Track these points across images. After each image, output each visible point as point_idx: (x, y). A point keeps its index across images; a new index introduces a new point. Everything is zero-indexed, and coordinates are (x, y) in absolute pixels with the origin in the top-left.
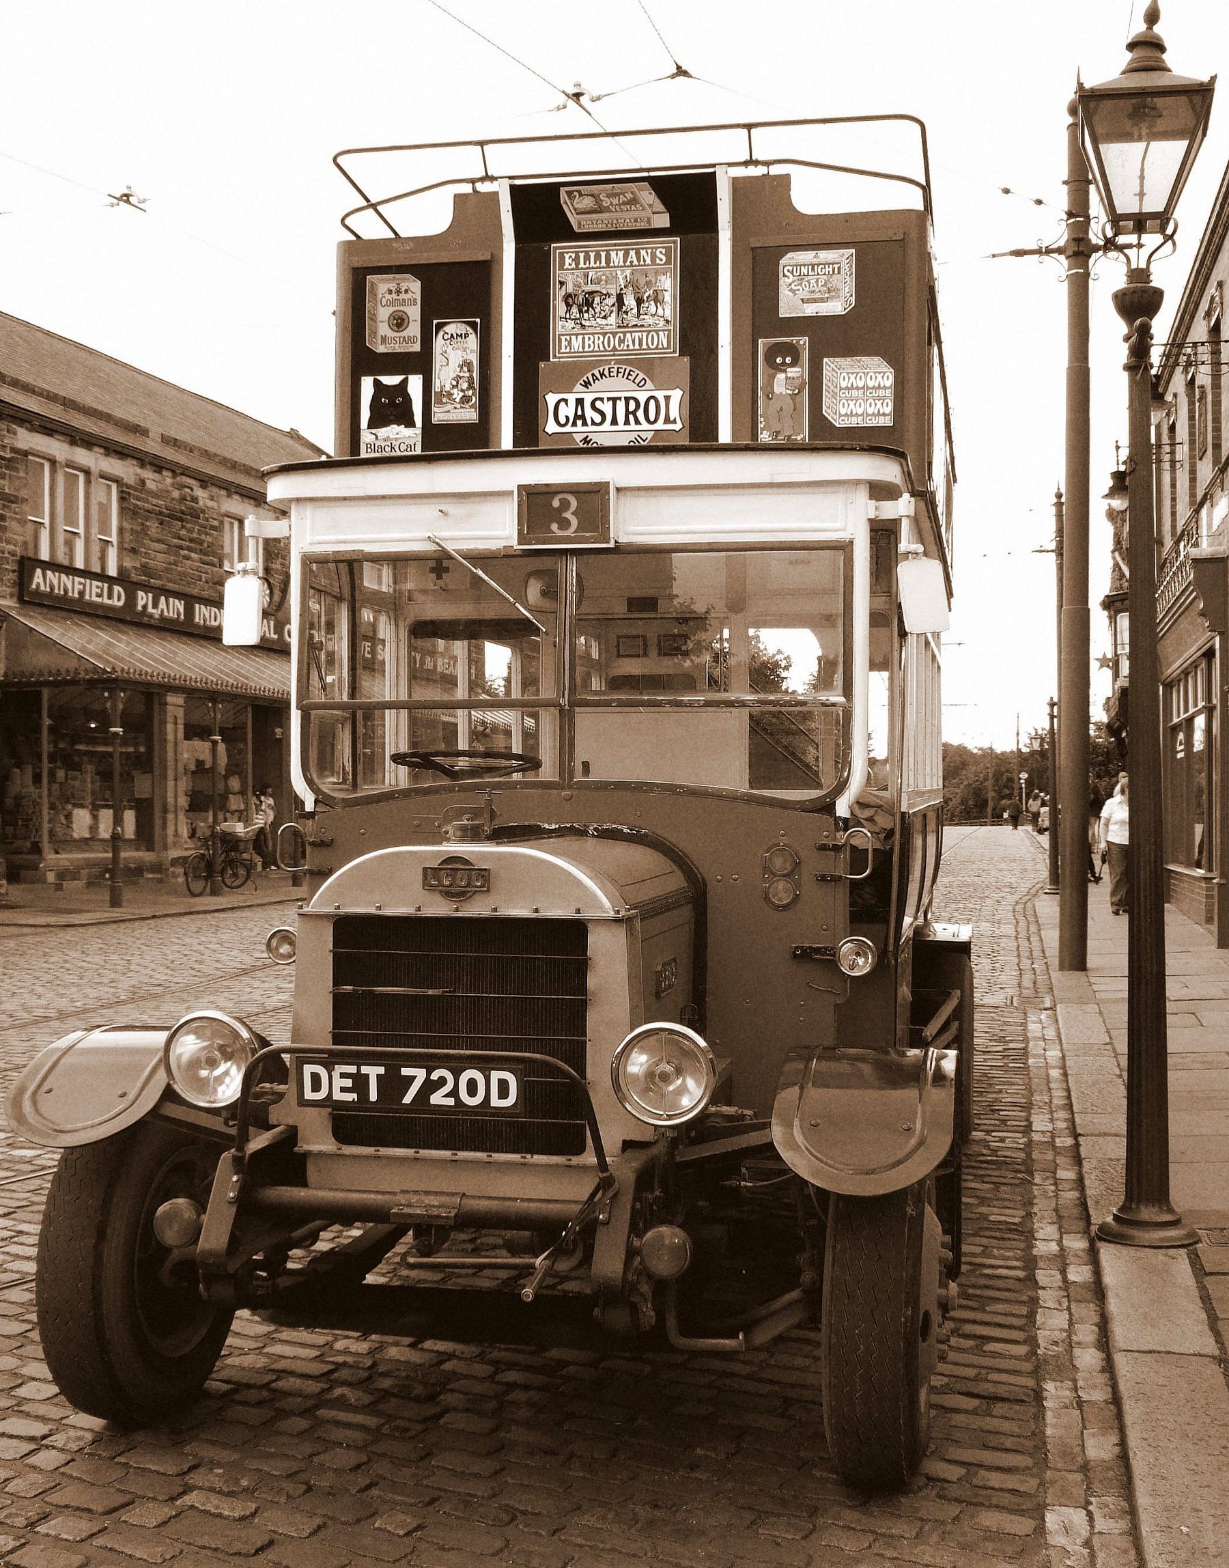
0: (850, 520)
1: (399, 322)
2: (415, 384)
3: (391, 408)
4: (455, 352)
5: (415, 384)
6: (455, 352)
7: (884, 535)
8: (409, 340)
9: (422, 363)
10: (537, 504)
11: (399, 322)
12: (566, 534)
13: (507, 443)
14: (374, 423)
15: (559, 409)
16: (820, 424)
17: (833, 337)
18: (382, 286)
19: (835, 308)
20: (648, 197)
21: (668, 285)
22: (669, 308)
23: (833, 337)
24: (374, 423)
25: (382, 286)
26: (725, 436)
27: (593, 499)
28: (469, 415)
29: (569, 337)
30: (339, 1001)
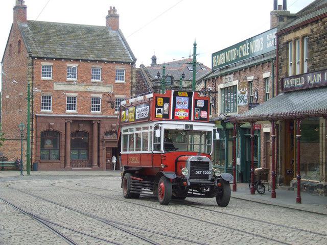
0: (211, 129)
1: (160, 103)
2: (162, 109)
3: (159, 112)
4: (166, 106)
5: (162, 109)
6: (166, 106)
7: (214, 130)
8: (161, 105)
9: (163, 107)
10: (186, 125)
11: (160, 103)
12: (189, 129)
13: (171, 118)
14: (158, 113)
15: (177, 114)
16: (200, 117)
17: (202, 109)
18: (159, 99)
19: (202, 106)
20: (186, 94)
21: (187, 102)
22: (187, 105)
23: (202, 109)
24: (158, 113)
25: (159, 99)
26: (192, 119)
27: (192, 126)
28: (167, 113)
29: (178, 106)
30: (191, 168)
